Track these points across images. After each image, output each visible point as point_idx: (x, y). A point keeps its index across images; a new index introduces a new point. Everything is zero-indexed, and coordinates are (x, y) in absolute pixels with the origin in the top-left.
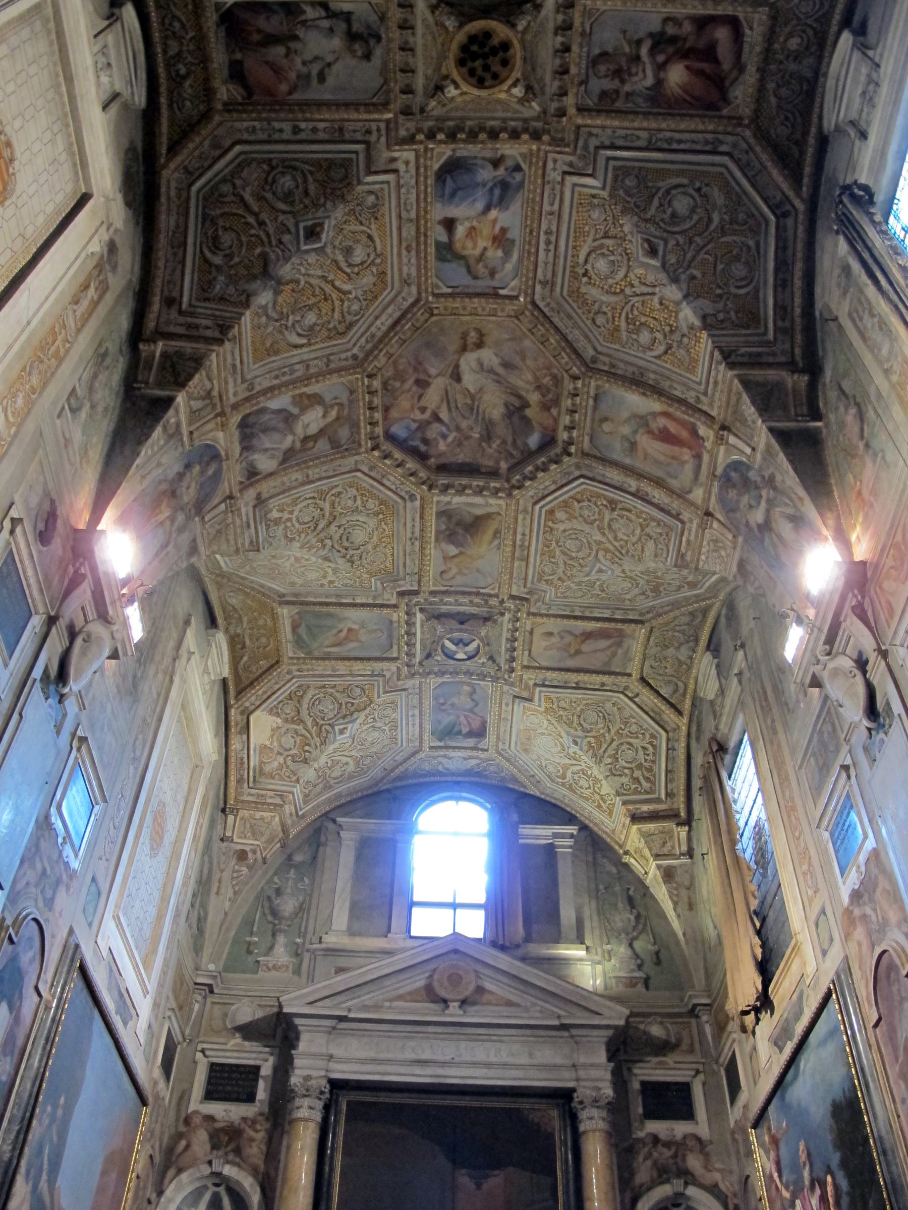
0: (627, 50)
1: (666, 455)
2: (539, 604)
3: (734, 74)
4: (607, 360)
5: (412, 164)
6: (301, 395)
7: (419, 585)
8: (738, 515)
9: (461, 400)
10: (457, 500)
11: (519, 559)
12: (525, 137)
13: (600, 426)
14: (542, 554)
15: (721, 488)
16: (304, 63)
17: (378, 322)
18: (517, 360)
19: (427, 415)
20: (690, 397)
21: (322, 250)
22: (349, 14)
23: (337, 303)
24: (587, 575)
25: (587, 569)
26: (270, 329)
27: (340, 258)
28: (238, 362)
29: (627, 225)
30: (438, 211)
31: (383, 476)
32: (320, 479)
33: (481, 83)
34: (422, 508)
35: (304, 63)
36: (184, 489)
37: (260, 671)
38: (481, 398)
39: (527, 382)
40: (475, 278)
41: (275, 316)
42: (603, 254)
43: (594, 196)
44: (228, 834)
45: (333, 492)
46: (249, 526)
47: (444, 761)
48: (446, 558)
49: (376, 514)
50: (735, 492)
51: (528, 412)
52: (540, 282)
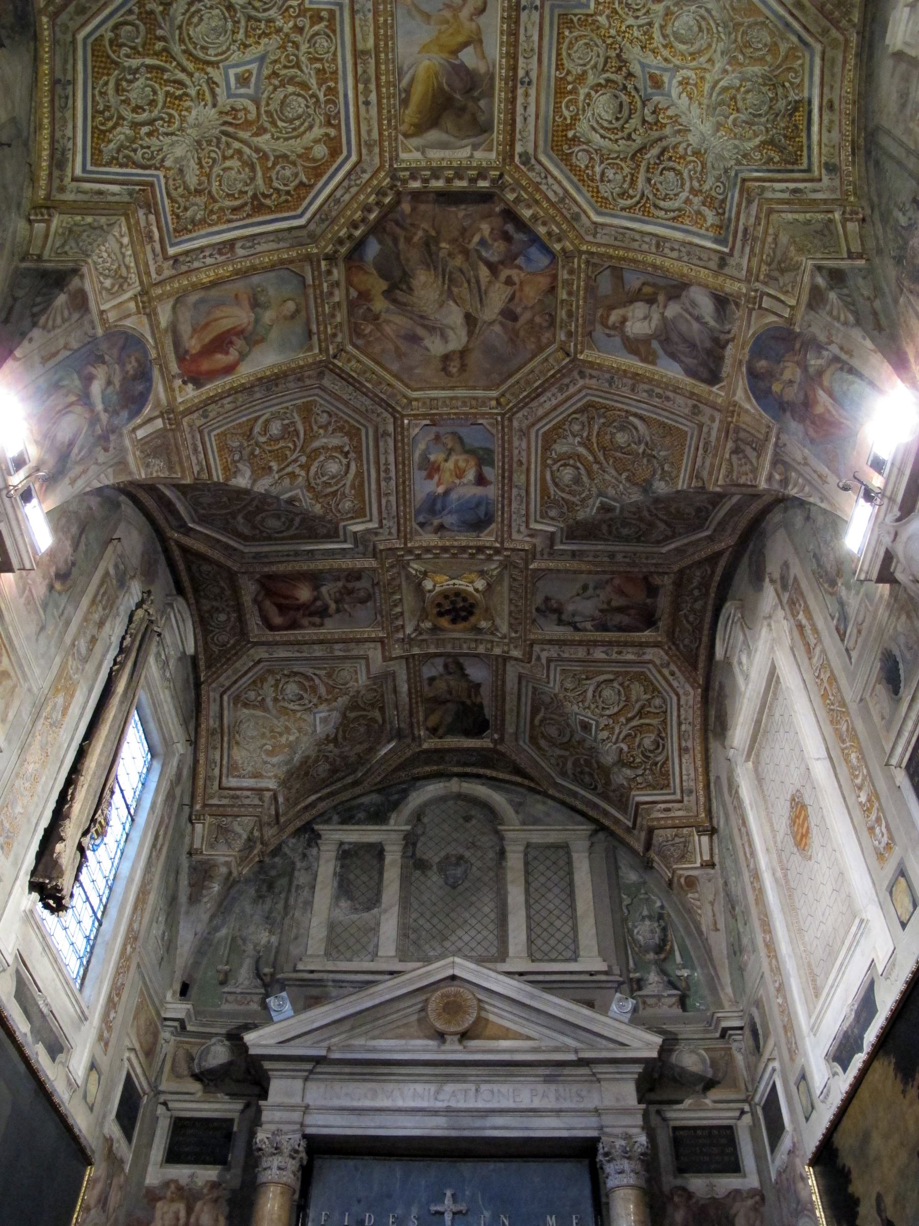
0: (346, 606)
1: (216, 320)
3: (260, 598)
4: (308, 382)
5: (514, 531)
6: (644, 360)
8: (115, 352)
9: (463, 291)
10: (461, 154)
12: (417, 552)
13: (297, 305)
14: (335, 72)
15: (145, 352)
16: (598, 596)
17: (554, 402)
18: (404, 346)
19: (505, 273)
20: (213, 409)
21: (600, 494)
22: (558, 625)
23: (594, 440)
24: (262, 59)
25: (266, 72)
26: (663, 453)
27: (585, 479)
28: (701, 451)
29: (318, 509)
30: (491, 492)
31: (562, 200)
32: (641, 232)
33: (458, 594)
35: (598, 596)
36: (796, 386)
38: (440, 295)
39: (388, 322)
40: (454, 434)
41: (655, 461)
42: (333, 477)
43: (352, 518)
46: (746, 230)
48: (475, 40)
49: (575, 140)
50: (131, 372)
51: (384, 285)
52: (389, 435)
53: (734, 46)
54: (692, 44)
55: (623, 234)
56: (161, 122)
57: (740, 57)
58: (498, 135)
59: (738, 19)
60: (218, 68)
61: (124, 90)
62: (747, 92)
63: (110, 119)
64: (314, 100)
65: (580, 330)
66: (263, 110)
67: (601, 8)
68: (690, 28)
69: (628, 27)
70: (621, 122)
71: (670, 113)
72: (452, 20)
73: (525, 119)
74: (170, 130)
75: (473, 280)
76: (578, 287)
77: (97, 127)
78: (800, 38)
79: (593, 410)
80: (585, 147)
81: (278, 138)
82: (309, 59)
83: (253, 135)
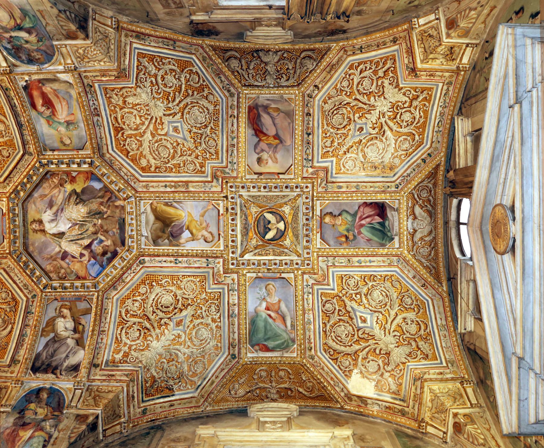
2: (227, 170)
7: (217, 257)
9: (76, 231)
11: (188, 188)
14: (179, 173)
17: (18, 282)
18: (47, 199)
24: (185, 139)
25: (179, 140)
34: (149, 255)
37: (312, 380)
38: (74, 220)
44: (441, 434)
45: (123, 314)
47: (418, 236)
48: (194, 238)
51: (79, 190)
53: (195, 356)
54: (195, 338)
55: (108, 313)
56: (157, 88)
57: (191, 360)
58: (152, 248)
59: (206, 357)
60: (181, 118)
61: (171, 73)
62: (176, 366)
63: (159, 65)
64: (167, 161)
65: (58, 294)
66: (162, 137)
67: (209, 295)
68: (202, 336)
69: (202, 308)
70: (161, 308)
71: (166, 331)
72: (202, 226)
73: (160, 262)
74: (154, 92)
75: (82, 236)
76: (80, 292)
77: (155, 58)
78: (200, 385)
79: (14, 304)
80: (149, 291)
81: (150, 143)
82: (184, 161)
83: (151, 131)
